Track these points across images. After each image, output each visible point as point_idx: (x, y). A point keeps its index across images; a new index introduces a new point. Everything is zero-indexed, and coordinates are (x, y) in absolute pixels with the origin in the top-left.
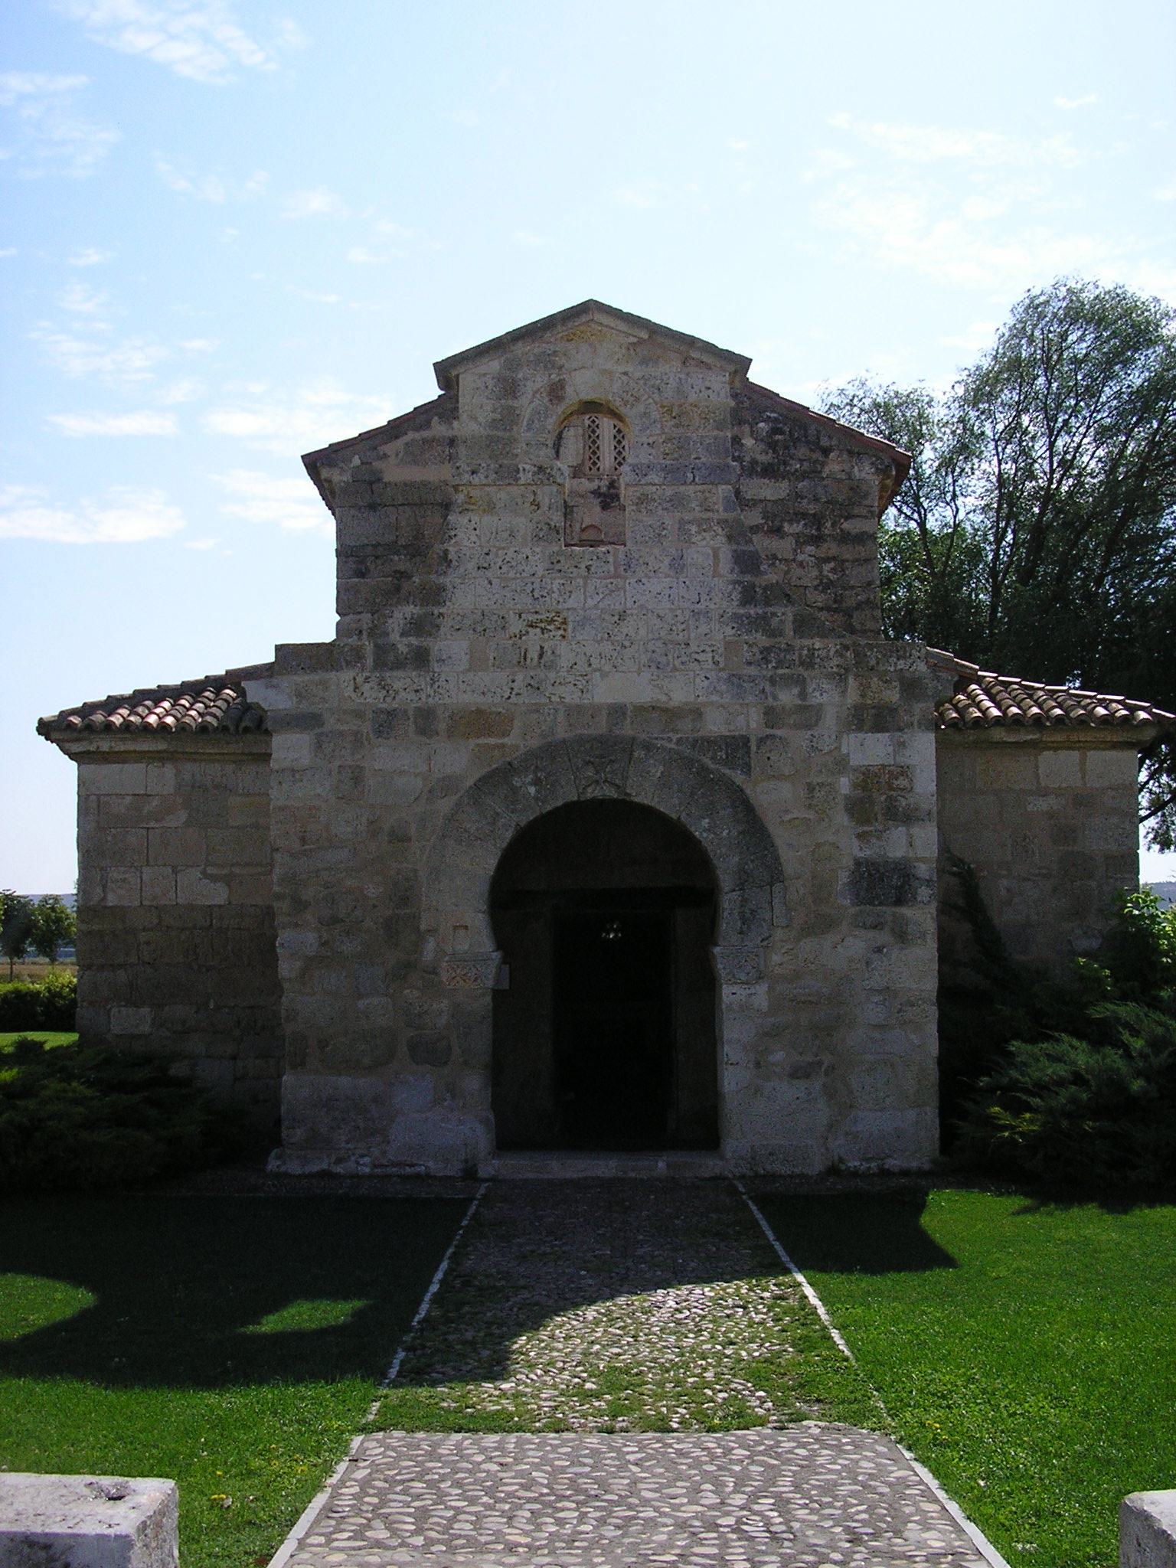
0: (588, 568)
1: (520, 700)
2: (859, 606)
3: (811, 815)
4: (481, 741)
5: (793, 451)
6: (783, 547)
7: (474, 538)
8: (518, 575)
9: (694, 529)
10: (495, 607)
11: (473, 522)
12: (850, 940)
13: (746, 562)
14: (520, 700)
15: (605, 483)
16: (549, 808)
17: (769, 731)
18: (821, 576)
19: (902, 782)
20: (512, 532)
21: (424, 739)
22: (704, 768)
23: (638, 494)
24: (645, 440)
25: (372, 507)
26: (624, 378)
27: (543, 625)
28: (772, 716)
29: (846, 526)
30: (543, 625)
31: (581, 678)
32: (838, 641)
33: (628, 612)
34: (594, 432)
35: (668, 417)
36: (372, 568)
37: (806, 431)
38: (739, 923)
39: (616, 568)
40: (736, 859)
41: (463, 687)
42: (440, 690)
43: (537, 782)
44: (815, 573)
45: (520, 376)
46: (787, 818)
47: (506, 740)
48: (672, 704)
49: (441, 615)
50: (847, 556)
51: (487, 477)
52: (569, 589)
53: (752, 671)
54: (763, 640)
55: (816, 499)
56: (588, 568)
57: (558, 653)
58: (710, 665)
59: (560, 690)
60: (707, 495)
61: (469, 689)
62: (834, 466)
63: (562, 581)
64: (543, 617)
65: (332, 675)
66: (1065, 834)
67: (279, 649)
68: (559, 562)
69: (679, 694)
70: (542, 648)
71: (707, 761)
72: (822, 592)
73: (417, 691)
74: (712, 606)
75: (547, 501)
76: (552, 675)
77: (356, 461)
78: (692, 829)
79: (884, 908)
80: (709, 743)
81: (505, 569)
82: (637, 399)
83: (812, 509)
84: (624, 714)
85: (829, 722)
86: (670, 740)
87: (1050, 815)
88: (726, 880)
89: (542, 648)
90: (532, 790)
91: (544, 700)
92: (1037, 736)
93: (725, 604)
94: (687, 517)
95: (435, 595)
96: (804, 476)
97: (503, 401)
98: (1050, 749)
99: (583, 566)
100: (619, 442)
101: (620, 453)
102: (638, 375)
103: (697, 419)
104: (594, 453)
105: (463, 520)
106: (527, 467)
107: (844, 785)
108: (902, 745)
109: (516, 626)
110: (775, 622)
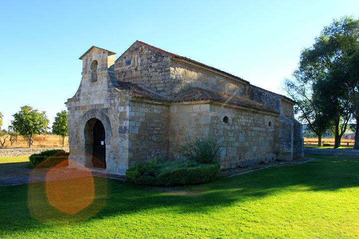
6: (157, 74)
62: (165, 59)
66: (197, 120)
67: (68, 99)
69: (102, 102)
80: (103, 109)
83: (161, 67)
85: (117, 105)
87: (195, 117)
108: (125, 108)
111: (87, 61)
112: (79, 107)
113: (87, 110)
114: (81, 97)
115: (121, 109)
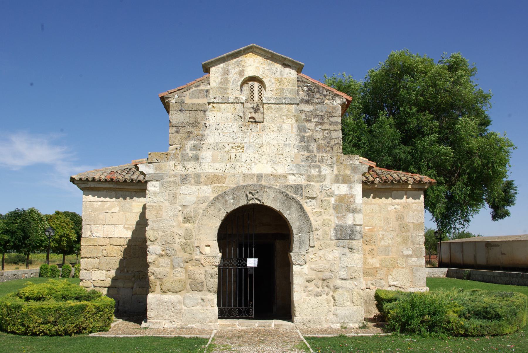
0: (251, 129)
1: (229, 171)
2: (335, 145)
3: (322, 210)
4: (216, 185)
5: (315, 96)
6: (312, 126)
7: (214, 120)
8: (228, 132)
9: (285, 118)
10: (221, 141)
11: (214, 114)
12: (335, 251)
13: (301, 129)
14: (229, 171)
15: (255, 105)
16: (238, 207)
17: (309, 183)
18: (323, 135)
19: (352, 200)
20: (226, 117)
21: (197, 184)
22: (287, 194)
23: (267, 106)
24: (270, 89)
25: (181, 111)
26: (263, 69)
27: (236, 148)
28: (309, 178)
29: (331, 119)
30: (236, 148)
31: (248, 165)
32: (331, 154)
33: (264, 144)
34: (252, 89)
35: (277, 82)
36: (181, 130)
37: (319, 89)
38: (299, 245)
39: (260, 130)
40: (298, 224)
41: (210, 167)
42: (202, 168)
43: (234, 198)
44: (321, 134)
45: (230, 68)
46: (314, 211)
47: (224, 185)
48: (277, 174)
49: (204, 144)
50: (331, 129)
51: (219, 100)
52: (244, 136)
53: (303, 163)
54: (307, 154)
55: (322, 111)
56: (251, 129)
57: (241, 157)
58: (290, 162)
59: (241, 169)
60: (290, 107)
61: (212, 168)
63: (243, 134)
64: (236, 145)
65: (168, 163)
68: (241, 127)
69: (280, 170)
70: (236, 155)
71: (288, 192)
72: (324, 140)
73: (195, 168)
74: (290, 142)
75: (238, 108)
76: (239, 164)
77: (176, 96)
78: (284, 214)
79: (345, 241)
81: (224, 129)
82: (267, 76)
83: (321, 114)
84: (262, 177)
86: (277, 186)
88: (295, 231)
89: (236, 155)
90: (232, 201)
91: (236, 172)
92: (392, 186)
93: (295, 141)
94: (283, 114)
95: (202, 138)
96: (318, 103)
97: (224, 76)
98: (395, 190)
99: (249, 129)
100: (260, 92)
101: (260, 96)
102: (268, 68)
103: (286, 82)
104: (252, 95)
105: (211, 114)
106: (232, 97)
107: (333, 200)
108: (351, 188)
109: (228, 148)
110: (311, 148)
111: (226, 72)
112: (198, 176)
113: (229, 184)
114: (206, 154)
115: (342, 189)
